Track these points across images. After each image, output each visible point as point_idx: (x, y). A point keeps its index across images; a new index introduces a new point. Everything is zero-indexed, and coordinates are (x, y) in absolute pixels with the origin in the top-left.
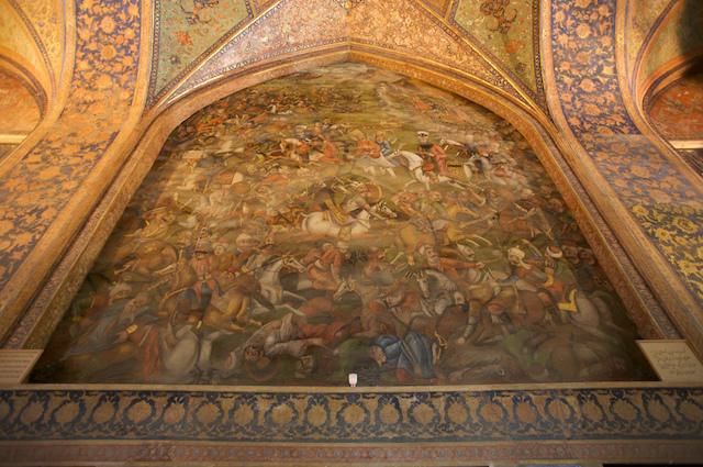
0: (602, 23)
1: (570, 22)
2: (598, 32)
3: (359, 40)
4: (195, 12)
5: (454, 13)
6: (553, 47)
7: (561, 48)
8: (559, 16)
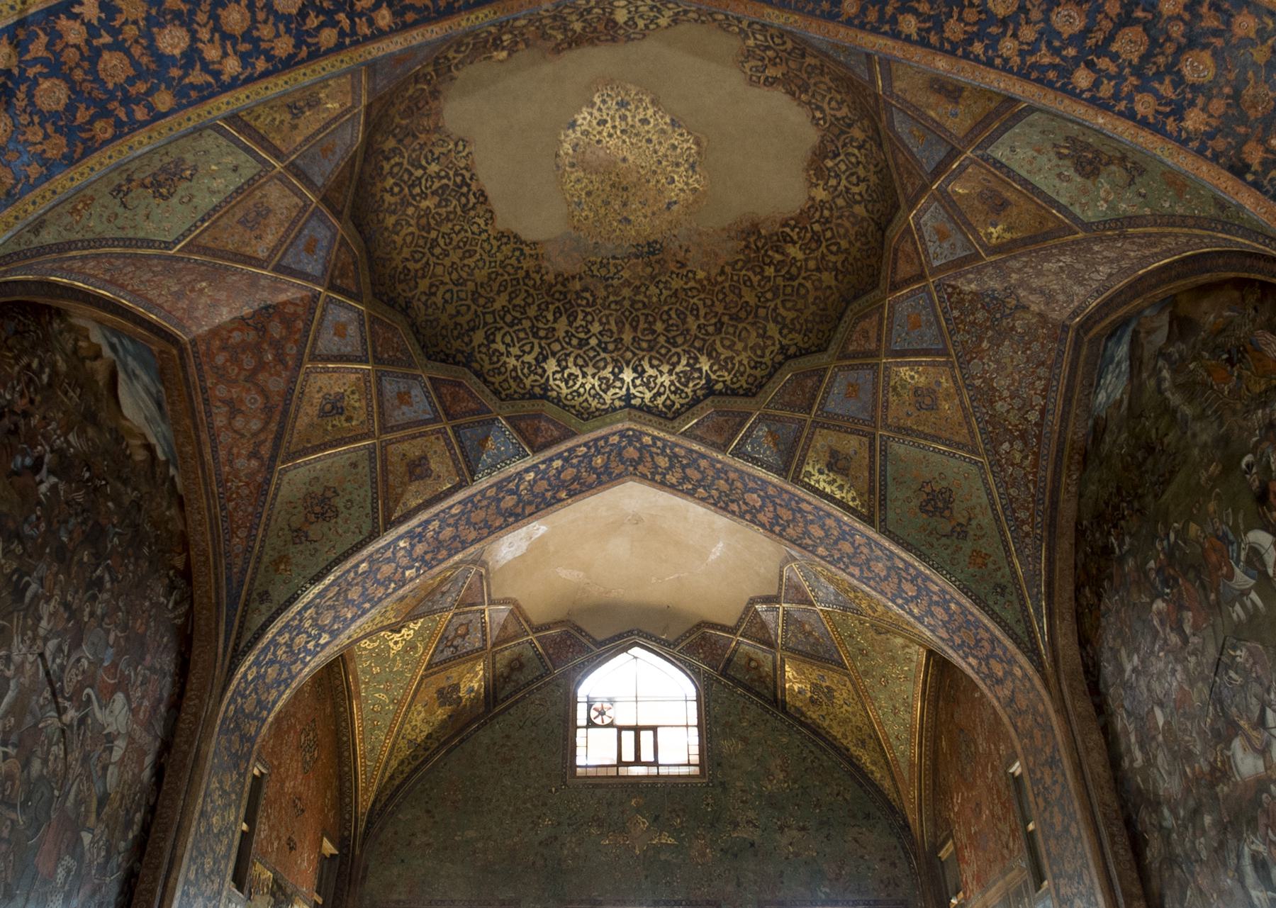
0: (1198, 17)
1: (1166, 89)
2: (1216, 33)
3: (1075, 314)
4: (954, 523)
5: (1075, 218)
6: (1200, 152)
7: (1211, 136)
8: (1144, 105)
